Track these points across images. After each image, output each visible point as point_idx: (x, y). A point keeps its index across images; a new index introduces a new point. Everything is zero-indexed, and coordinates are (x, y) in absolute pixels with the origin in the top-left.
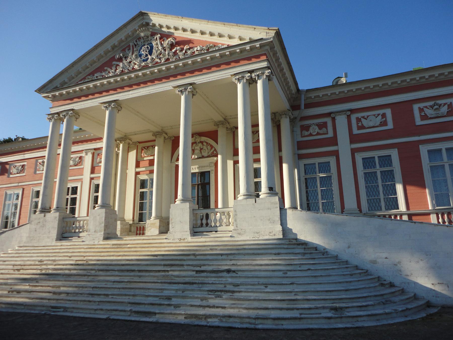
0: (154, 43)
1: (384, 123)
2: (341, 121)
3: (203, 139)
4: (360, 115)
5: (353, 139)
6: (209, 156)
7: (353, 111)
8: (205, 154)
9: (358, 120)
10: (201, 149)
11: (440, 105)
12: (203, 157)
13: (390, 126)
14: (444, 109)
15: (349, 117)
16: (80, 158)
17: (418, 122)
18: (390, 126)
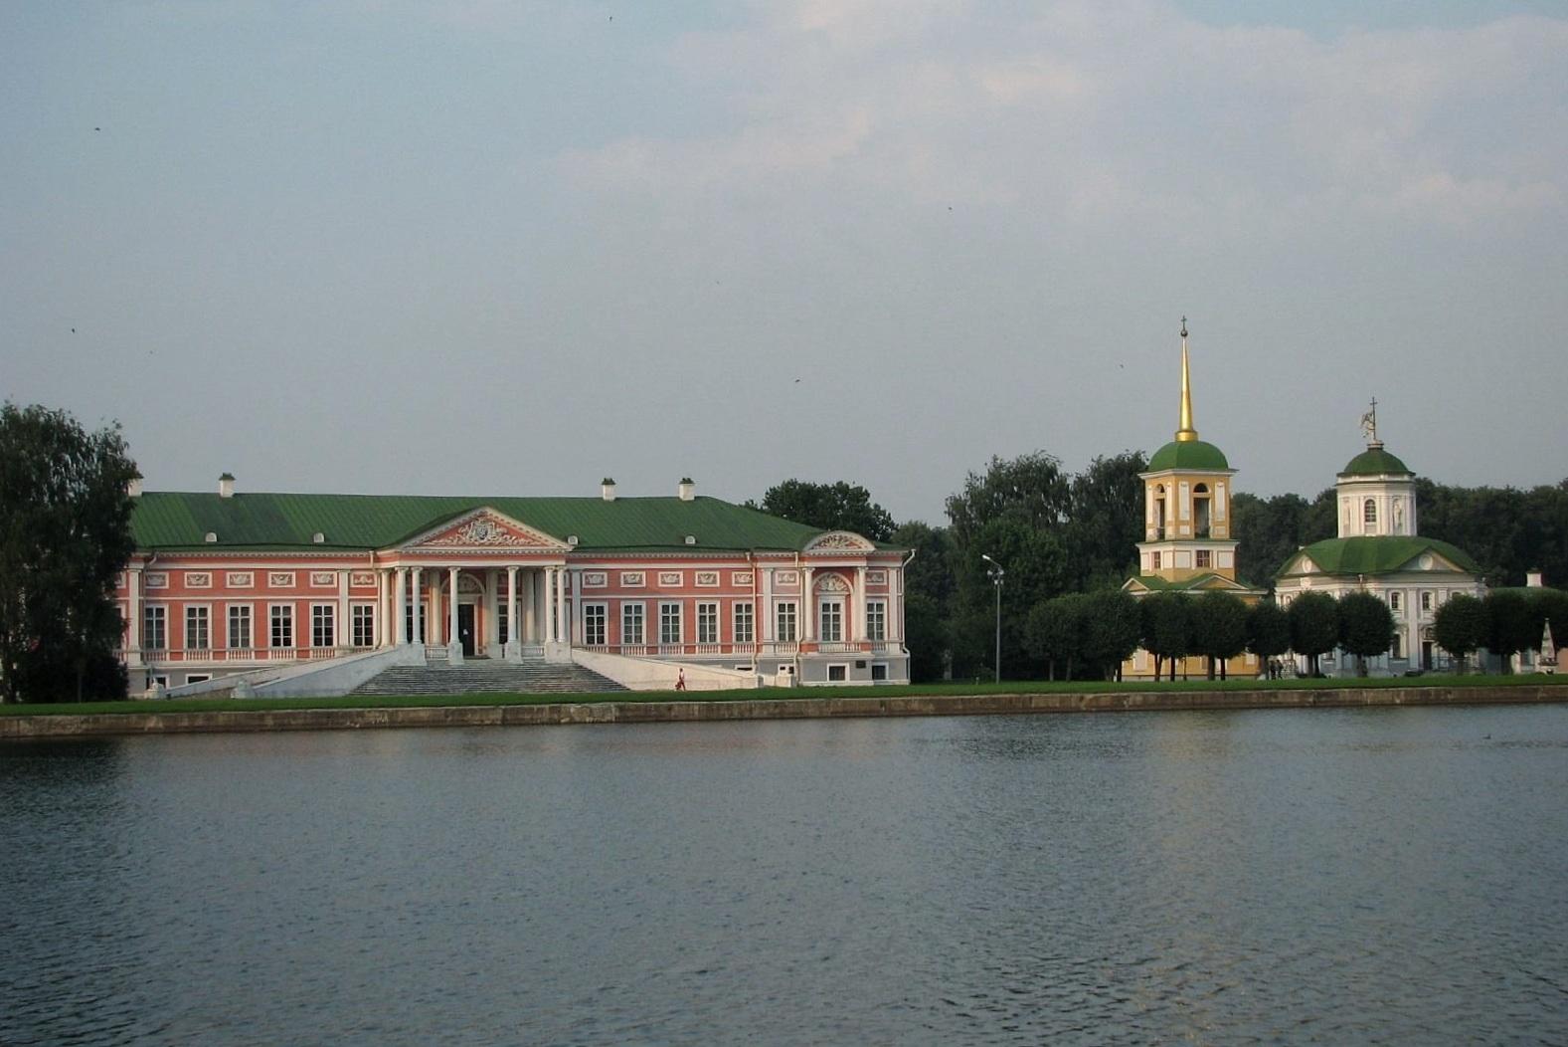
0: (489, 527)
1: (602, 583)
2: (576, 576)
3: (467, 575)
4: (589, 573)
5: (583, 591)
6: (473, 592)
7: (586, 570)
8: (470, 589)
9: (586, 577)
10: (465, 585)
11: (635, 575)
12: (467, 592)
13: (605, 585)
14: (638, 578)
15: (581, 575)
16: (332, 576)
17: (623, 586)
18: (605, 585)
